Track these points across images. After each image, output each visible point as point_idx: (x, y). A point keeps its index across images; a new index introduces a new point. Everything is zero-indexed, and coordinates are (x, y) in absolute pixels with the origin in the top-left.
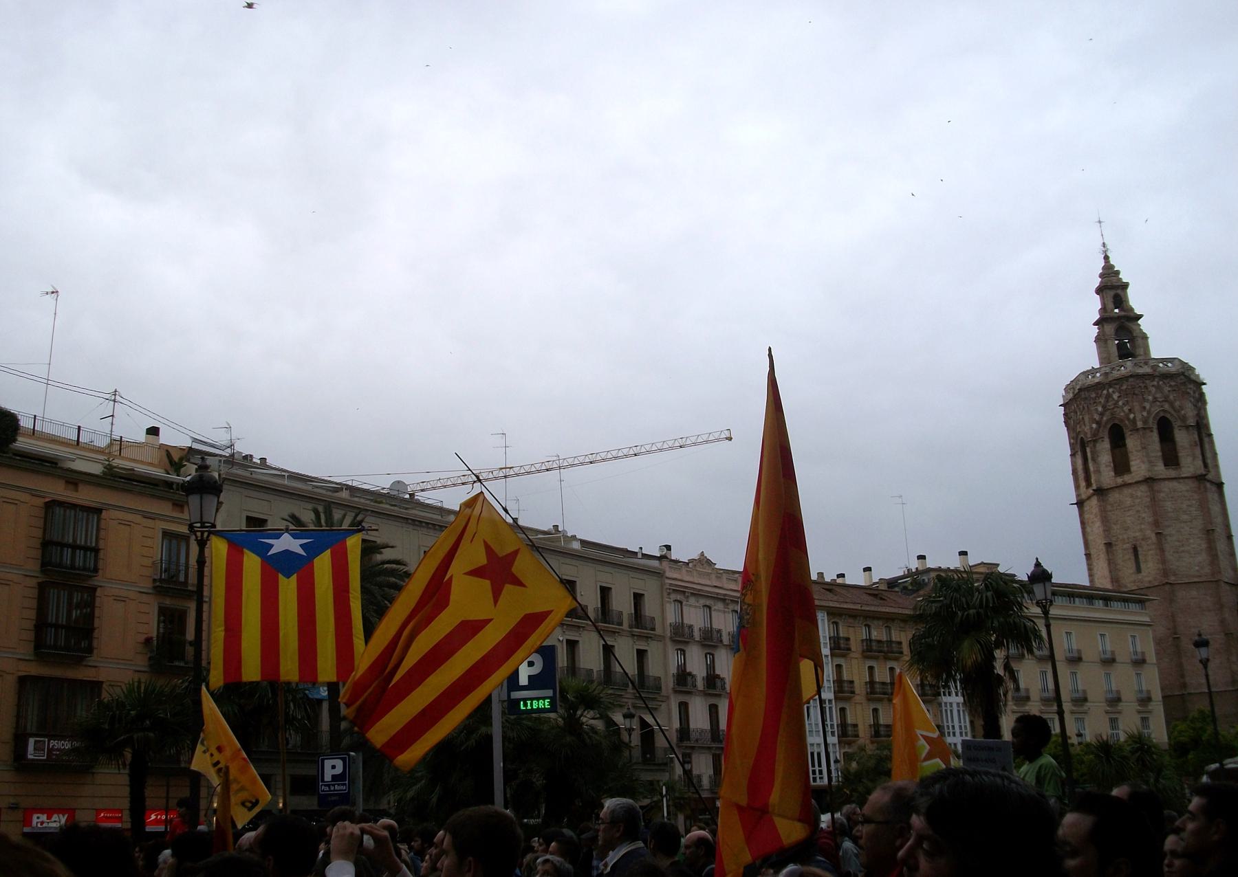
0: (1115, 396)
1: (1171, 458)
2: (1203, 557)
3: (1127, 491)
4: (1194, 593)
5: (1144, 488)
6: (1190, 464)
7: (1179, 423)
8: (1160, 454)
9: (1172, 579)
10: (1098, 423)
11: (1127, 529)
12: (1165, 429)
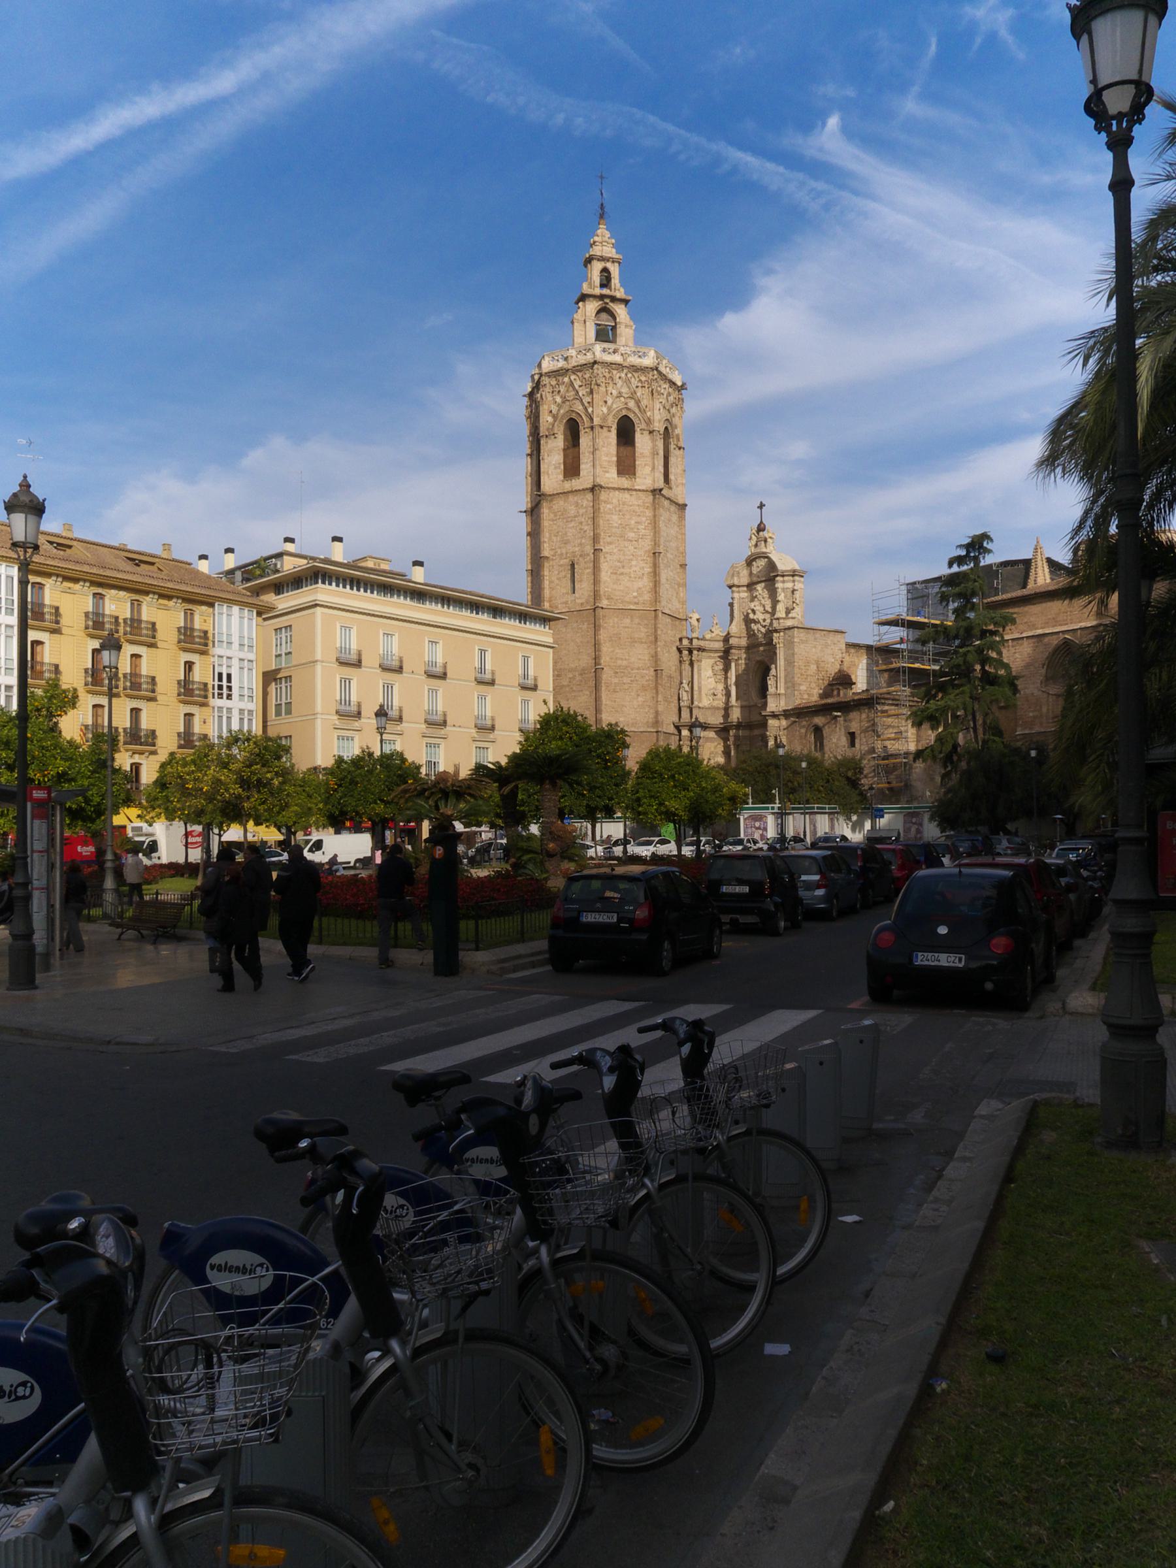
0: (577, 384)
1: (626, 467)
2: (646, 583)
3: (571, 498)
4: (627, 621)
5: (589, 496)
7: (643, 426)
8: (615, 459)
9: (604, 603)
10: (555, 417)
11: (566, 543)
12: (626, 432)
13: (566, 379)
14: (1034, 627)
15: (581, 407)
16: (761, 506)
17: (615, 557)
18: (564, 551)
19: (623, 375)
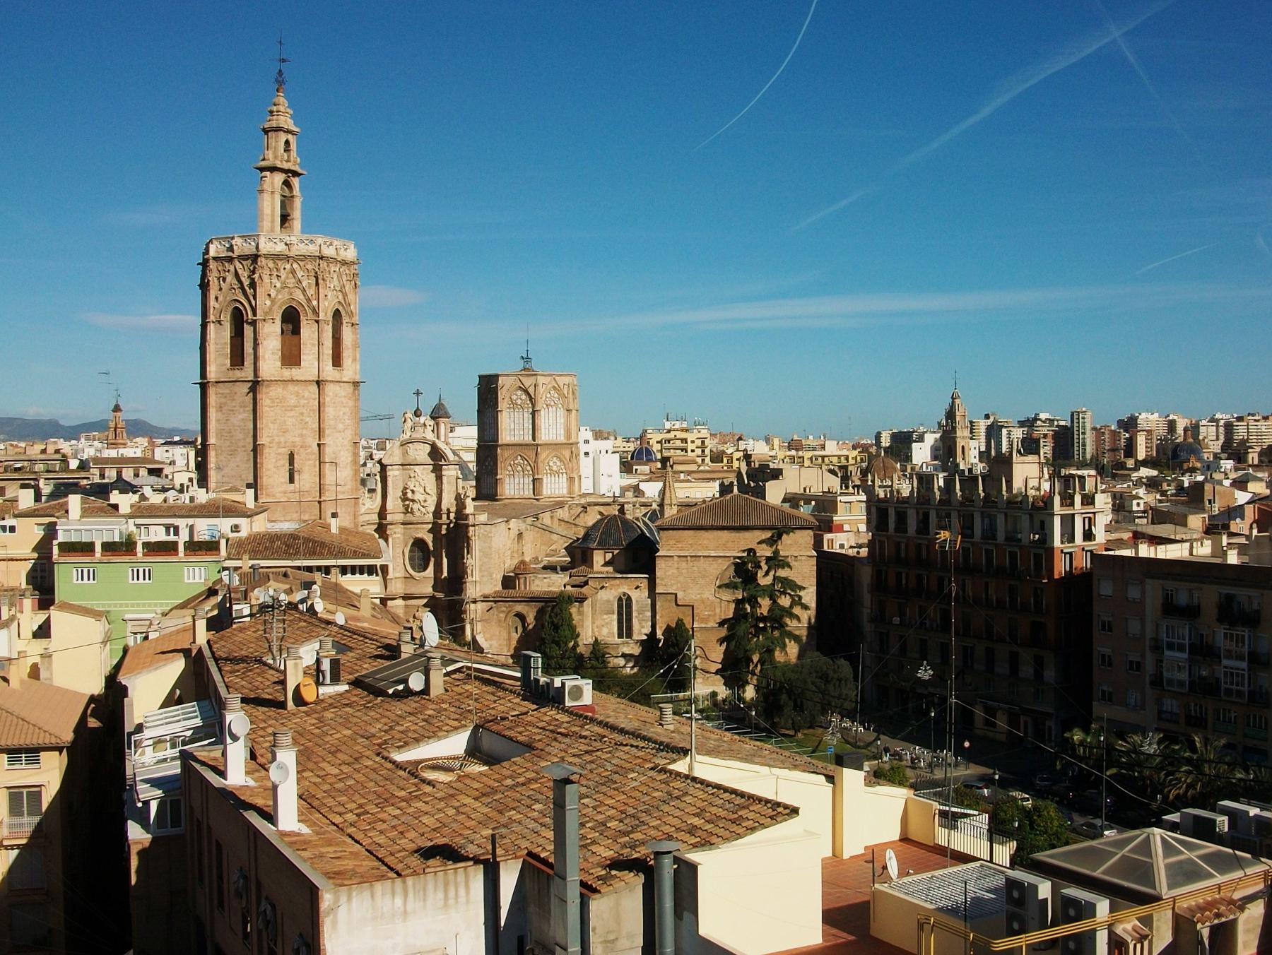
0: (300, 274)
3: (291, 387)
10: (273, 302)
13: (288, 266)
14: (707, 548)
15: (302, 297)
16: (418, 393)
18: (282, 439)
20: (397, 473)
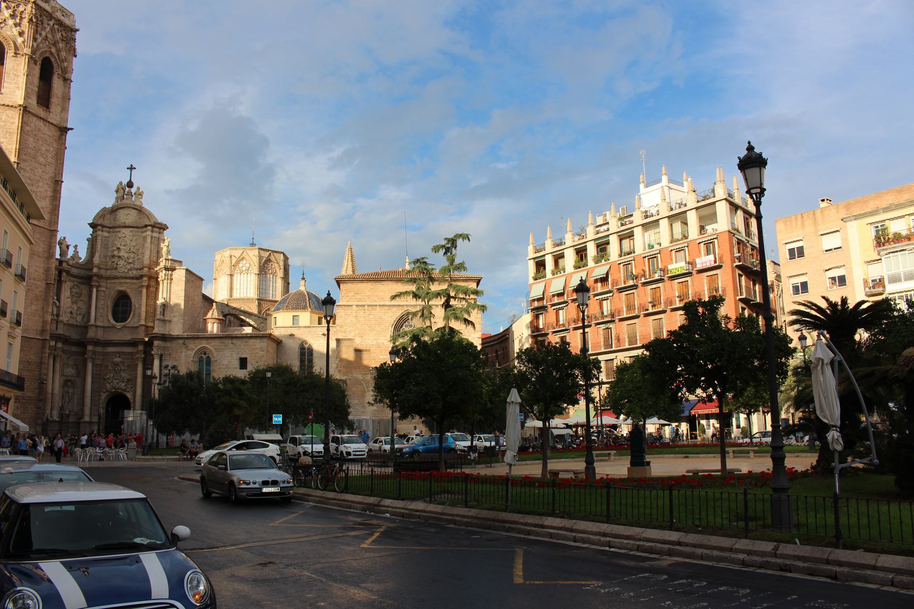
6: (54, 116)
7: (60, 72)
8: (36, 89)
16: (131, 168)
17: (27, 175)
19: (51, 23)
20: (106, 234)
